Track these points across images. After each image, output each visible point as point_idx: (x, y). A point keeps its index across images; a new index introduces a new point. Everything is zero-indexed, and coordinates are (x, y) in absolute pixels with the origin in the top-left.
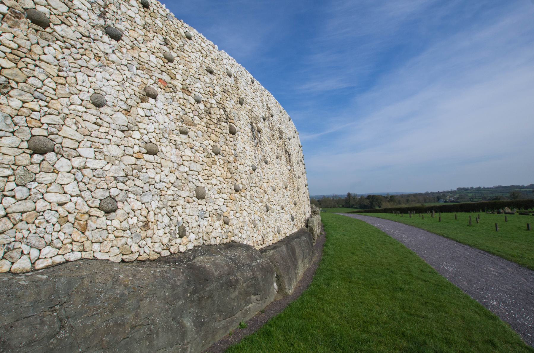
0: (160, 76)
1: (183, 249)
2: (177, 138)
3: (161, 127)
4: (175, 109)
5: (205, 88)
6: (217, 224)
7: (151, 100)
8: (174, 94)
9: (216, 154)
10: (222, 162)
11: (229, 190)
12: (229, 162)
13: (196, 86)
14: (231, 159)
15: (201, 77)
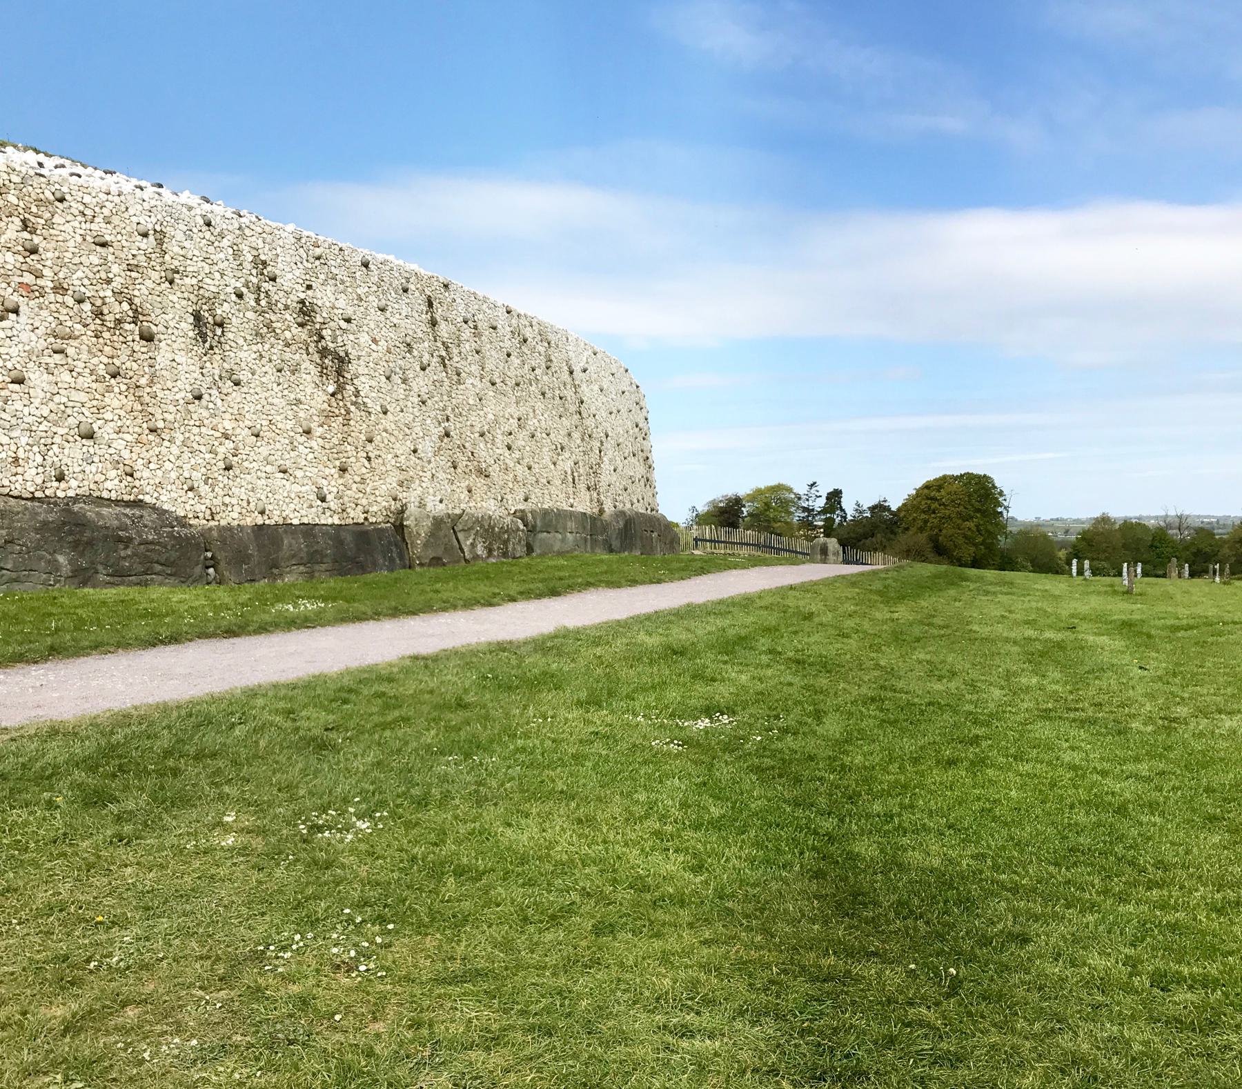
0: (21, 280)
1: (60, 494)
2: (48, 360)
3: (27, 348)
4: (46, 320)
5: (91, 275)
6: (113, 474)
7: (12, 316)
8: (41, 300)
9: (114, 376)
10: (124, 388)
11: (137, 429)
12: (138, 387)
13: (75, 277)
14: (143, 381)
15: (83, 259)
